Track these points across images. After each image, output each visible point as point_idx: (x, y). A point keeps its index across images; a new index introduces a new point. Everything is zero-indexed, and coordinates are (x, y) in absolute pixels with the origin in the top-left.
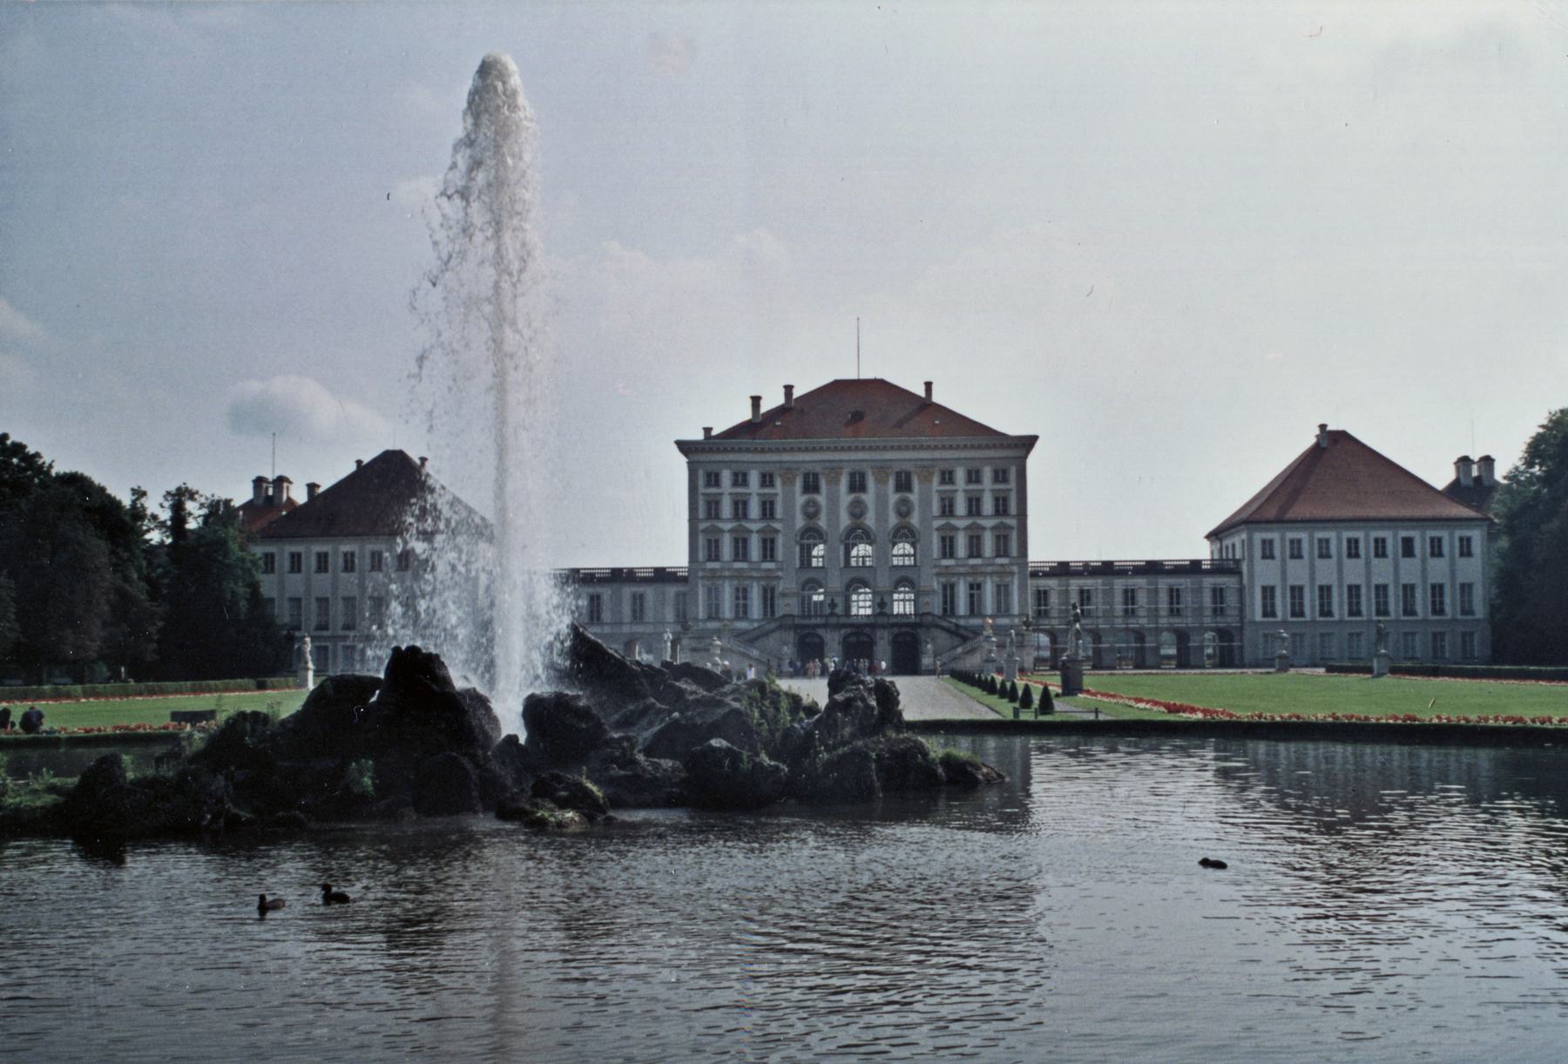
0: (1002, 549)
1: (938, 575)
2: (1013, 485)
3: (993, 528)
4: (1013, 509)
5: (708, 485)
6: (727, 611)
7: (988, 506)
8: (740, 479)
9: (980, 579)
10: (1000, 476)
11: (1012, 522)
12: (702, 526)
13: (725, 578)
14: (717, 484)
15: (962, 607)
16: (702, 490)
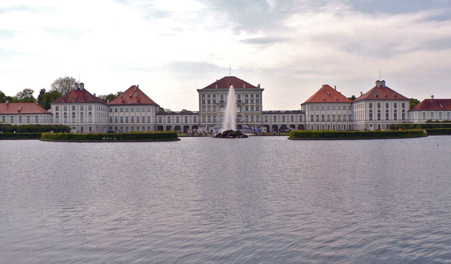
0: (257, 110)
1: (244, 114)
2: (259, 97)
3: (256, 106)
4: (260, 102)
5: (203, 97)
6: (207, 121)
7: (255, 101)
8: (209, 96)
9: (253, 115)
10: (257, 96)
11: (260, 105)
12: (202, 105)
13: (206, 115)
14: (204, 97)
15: (250, 120)
16: (201, 98)
